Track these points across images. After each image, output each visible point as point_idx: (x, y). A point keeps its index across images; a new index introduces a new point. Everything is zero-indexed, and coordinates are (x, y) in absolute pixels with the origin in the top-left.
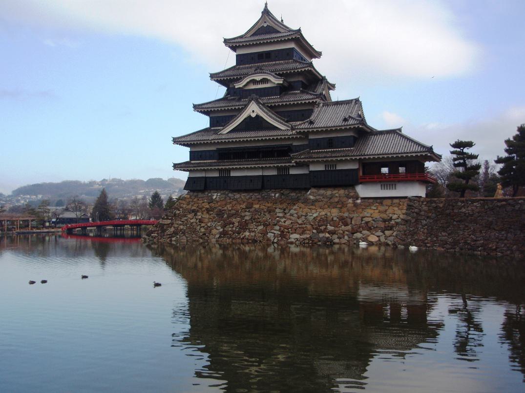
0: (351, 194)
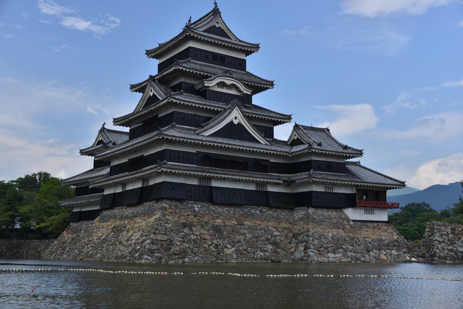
0: (343, 216)
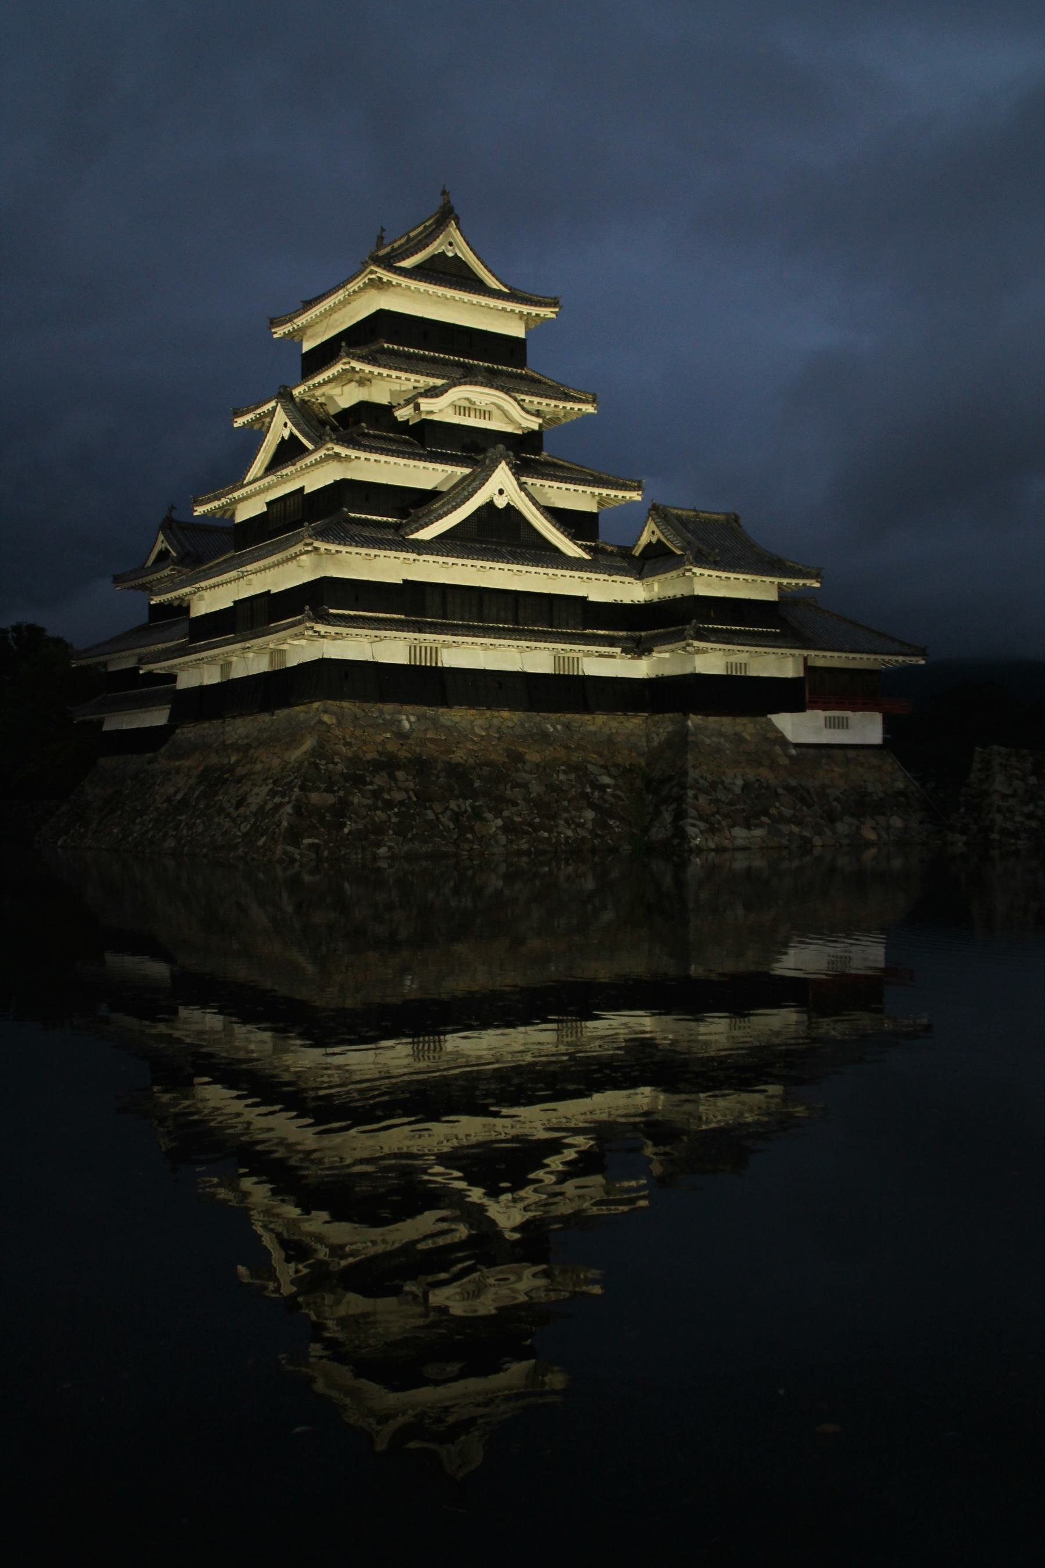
0: (771, 735)
